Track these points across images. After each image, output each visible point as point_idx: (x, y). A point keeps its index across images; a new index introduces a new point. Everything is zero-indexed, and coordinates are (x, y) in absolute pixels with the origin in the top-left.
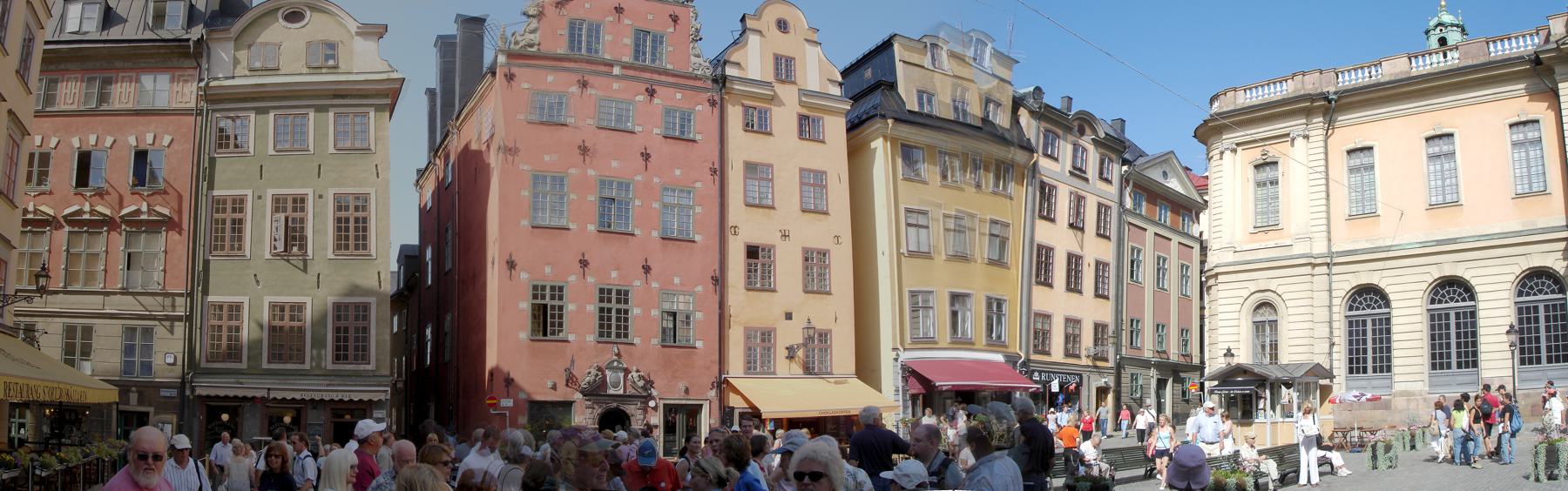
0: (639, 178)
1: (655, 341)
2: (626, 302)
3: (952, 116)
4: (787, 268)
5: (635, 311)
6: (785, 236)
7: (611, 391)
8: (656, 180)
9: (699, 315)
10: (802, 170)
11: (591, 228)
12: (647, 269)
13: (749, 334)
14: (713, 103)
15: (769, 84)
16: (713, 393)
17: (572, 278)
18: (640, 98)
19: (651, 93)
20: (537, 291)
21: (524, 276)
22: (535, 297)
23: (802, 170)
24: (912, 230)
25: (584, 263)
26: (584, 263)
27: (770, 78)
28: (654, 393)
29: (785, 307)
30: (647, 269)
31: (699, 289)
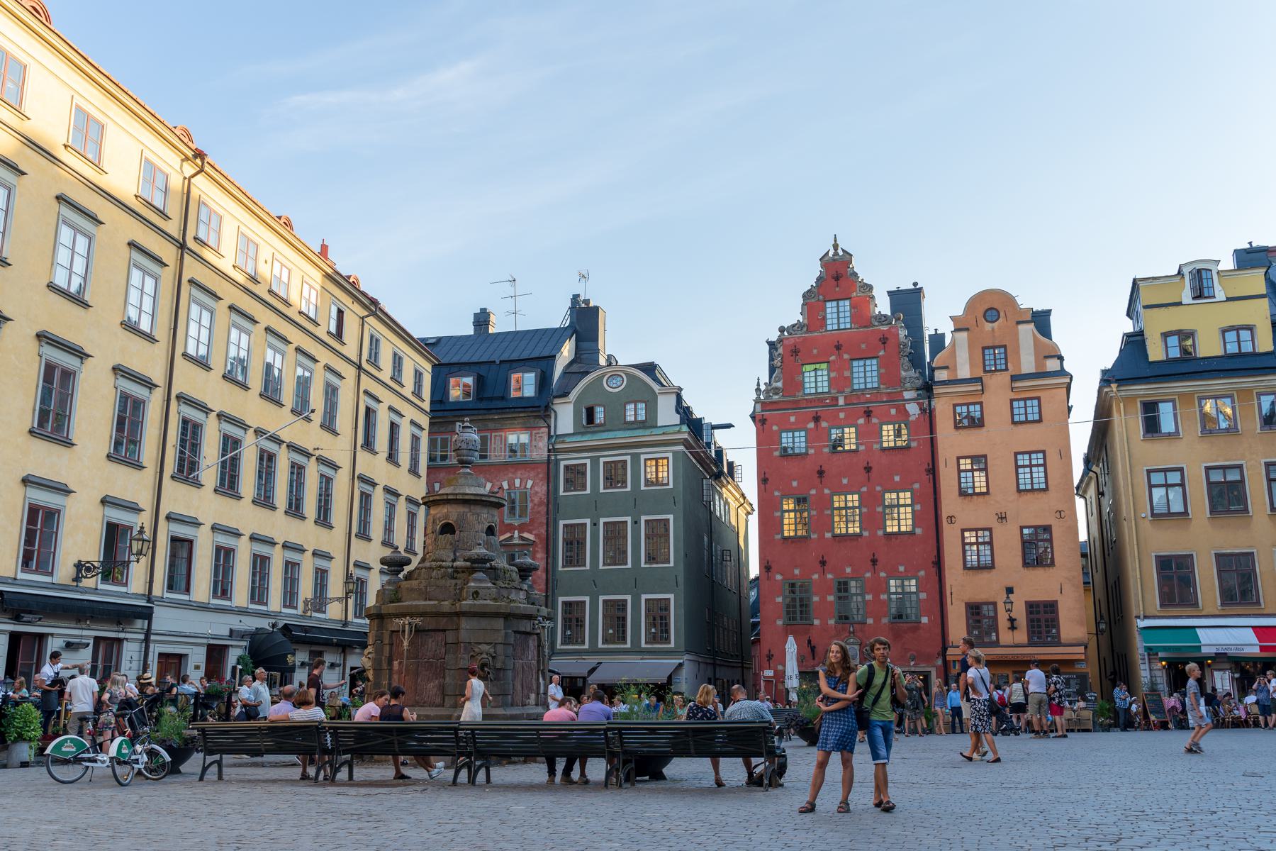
0: (864, 489)
1: (885, 620)
3: (1219, 352)
6: (1002, 518)
8: (878, 488)
9: (923, 596)
10: (1016, 454)
11: (828, 535)
12: (874, 562)
13: (974, 610)
15: (981, 379)
16: (940, 662)
18: (861, 421)
19: (868, 414)
21: (779, 577)
23: (1016, 454)
24: (1158, 493)
25: (823, 563)
26: (823, 563)
27: (980, 373)
30: (874, 562)
31: (922, 573)
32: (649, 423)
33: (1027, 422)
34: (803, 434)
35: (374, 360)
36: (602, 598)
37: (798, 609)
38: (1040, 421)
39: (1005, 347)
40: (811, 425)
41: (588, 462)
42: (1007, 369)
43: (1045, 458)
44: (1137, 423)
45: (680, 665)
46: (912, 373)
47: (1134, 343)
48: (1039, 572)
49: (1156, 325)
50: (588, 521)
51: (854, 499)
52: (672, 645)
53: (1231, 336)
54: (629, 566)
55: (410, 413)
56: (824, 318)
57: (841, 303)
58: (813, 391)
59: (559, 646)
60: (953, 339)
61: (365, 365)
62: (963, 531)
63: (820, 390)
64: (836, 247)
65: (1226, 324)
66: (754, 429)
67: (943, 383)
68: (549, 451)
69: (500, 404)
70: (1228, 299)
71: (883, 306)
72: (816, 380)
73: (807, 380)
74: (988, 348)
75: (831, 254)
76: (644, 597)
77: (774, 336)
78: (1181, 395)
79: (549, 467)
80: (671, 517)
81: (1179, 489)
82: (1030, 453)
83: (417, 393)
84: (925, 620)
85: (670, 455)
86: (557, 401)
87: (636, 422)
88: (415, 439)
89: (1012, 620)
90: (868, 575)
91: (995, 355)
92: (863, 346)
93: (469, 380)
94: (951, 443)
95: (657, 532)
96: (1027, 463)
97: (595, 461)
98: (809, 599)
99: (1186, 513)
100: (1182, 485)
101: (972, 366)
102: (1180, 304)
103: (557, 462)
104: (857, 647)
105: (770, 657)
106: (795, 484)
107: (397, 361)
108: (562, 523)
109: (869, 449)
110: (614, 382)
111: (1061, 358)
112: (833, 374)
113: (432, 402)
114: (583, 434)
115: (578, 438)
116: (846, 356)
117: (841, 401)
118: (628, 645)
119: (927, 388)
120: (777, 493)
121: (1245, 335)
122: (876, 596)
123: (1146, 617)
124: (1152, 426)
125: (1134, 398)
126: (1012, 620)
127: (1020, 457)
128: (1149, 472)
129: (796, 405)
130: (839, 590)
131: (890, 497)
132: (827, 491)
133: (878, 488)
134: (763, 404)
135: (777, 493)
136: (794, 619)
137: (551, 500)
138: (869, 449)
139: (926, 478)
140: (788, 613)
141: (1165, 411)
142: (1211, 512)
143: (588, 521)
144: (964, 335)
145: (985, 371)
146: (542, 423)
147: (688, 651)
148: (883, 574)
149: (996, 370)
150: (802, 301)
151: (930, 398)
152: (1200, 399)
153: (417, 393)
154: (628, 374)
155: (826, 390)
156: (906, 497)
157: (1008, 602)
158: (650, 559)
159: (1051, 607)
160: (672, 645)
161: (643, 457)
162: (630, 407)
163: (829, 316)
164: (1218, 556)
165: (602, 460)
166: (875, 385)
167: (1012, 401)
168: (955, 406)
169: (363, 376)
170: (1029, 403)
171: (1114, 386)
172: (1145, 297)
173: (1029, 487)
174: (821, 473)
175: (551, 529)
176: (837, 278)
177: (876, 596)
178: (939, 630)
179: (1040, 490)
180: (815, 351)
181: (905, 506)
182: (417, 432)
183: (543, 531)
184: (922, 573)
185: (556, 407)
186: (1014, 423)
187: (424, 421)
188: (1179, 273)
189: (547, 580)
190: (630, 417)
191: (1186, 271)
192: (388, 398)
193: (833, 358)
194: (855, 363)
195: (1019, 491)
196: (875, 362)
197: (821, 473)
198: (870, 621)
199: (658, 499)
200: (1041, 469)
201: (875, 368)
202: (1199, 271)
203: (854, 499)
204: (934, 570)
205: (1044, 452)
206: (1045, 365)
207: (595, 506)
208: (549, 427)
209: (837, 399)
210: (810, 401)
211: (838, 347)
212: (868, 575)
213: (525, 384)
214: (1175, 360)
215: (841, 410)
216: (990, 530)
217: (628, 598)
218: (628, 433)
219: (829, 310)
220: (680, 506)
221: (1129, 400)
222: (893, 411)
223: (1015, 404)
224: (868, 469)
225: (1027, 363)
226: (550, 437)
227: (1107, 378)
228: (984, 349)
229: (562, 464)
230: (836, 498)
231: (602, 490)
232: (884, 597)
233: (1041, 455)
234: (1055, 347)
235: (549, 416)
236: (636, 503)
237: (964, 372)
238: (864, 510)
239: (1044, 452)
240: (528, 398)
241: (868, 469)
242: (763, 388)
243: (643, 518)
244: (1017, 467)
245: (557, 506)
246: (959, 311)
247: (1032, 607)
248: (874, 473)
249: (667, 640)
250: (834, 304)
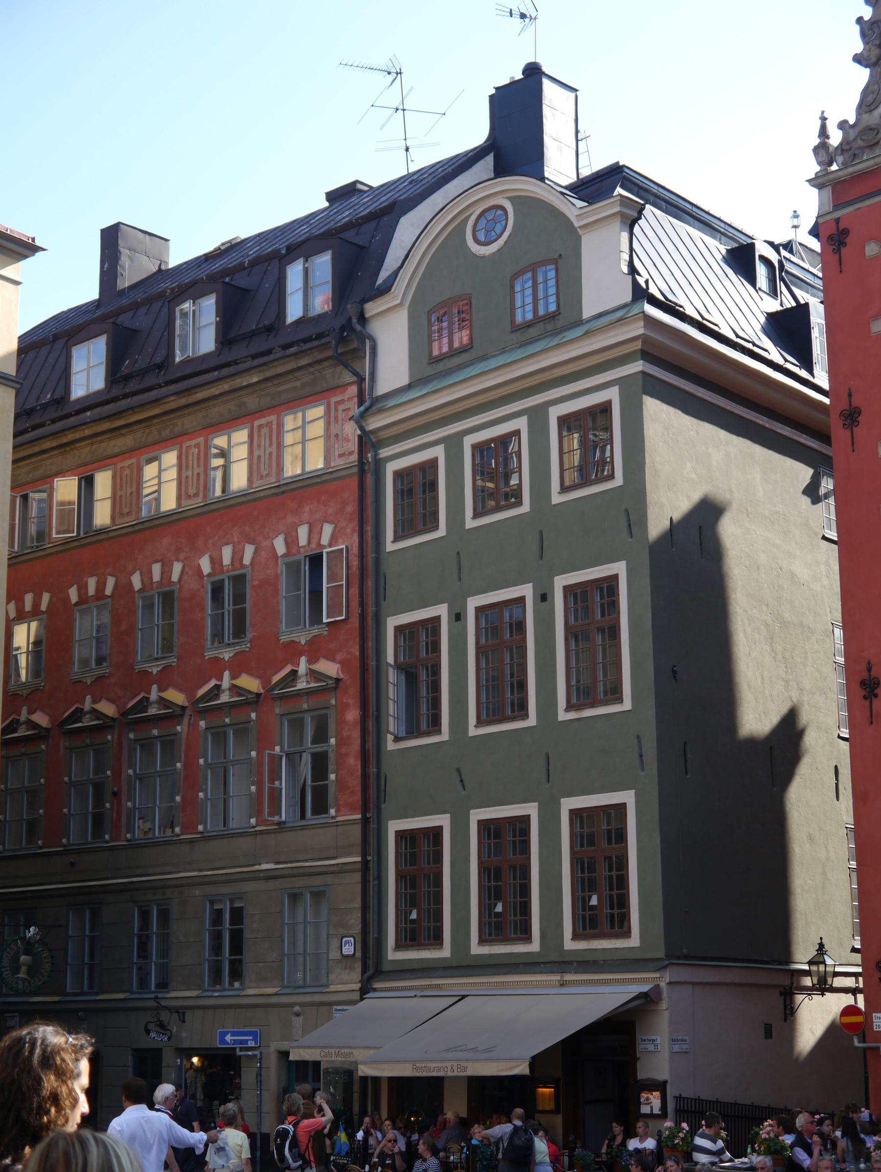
52: (634, 941)
59: (393, 955)
118: (535, 946)
143: (442, 611)
158: (582, 696)
160: (634, 941)
161: (555, 413)
189: (365, 776)
217: (531, 809)
242: (836, 138)
249: (619, 925)
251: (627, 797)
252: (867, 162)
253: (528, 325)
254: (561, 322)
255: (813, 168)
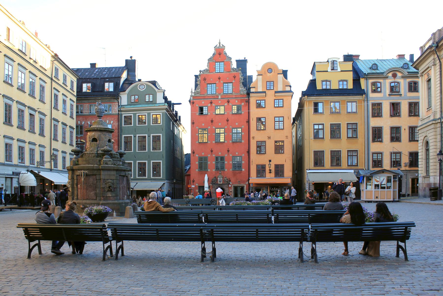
0: (226, 127)
1: (231, 170)
2: (223, 160)
4: (270, 147)
5: (226, 162)
6: (269, 138)
7: (219, 183)
8: (231, 127)
11: (214, 142)
12: (228, 151)
14: (246, 102)
16: (247, 183)
17: (209, 155)
18: (226, 104)
19: (228, 102)
20: (201, 159)
21: (197, 156)
22: (200, 160)
23: (275, 117)
25: (212, 151)
26: (212, 151)
27: (265, 90)
28: (231, 183)
29: (270, 158)
30: (228, 151)
31: (243, 155)
32: (154, 102)
33: (279, 107)
34: (206, 108)
35: (56, 77)
36: (137, 162)
37: (203, 166)
38: (283, 107)
39: (273, 82)
40: (209, 105)
41: (132, 115)
42: (273, 89)
43: (283, 119)
44: (312, 108)
45: (164, 184)
46: (243, 89)
47: (313, 83)
48: (279, 155)
49: (319, 78)
50: (132, 135)
51: (222, 130)
53: (341, 83)
54: (147, 151)
55: (70, 96)
56: (215, 68)
57: (221, 63)
58: (210, 93)
60: (257, 80)
61: (54, 78)
62: (257, 142)
63: (213, 93)
64: (220, 43)
65: (340, 79)
66: (190, 106)
67: (253, 92)
68: (119, 111)
69: (102, 93)
70: (341, 71)
71: (234, 65)
72: (211, 90)
73: (208, 89)
74: (268, 82)
75: (218, 46)
76: (152, 161)
77: (198, 74)
78: (325, 101)
79: (119, 116)
80: (161, 135)
81: (322, 130)
82: (279, 117)
83: (72, 89)
84: (243, 170)
85: (161, 113)
86: (121, 93)
87: (149, 101)
88: (72, 106)
89: (270, 170)
90: (226, 155)
91: (270, 84)
92: (228, 79)
93: (89, 85)
94: (255, 113)
95: (156, 139)
96: (278, 120)
97: (135, 115)
98: (206, 163)
99: (323, 138)
100: (323, 129)
101: (263, 87)
102: (327, 71)
103: (121, 115)
104: (222, 178)
105: (193, 181)
106: (203, 125)
107: (65, 77)
108: (123, 136)
109: (228, 113)
110: (142, 87)
111: (290, 86)
112: (217, 88)
113: (77, 92)
114: (131, 105)
115: (129, 107)
116: (222, 82)
117: (220, 97)
119: (248, 94)
120: (197, 128)
121: (345, 83)
122: (228, 162)
123: (309, 170)
124: (316, 110)
125: (311, 101)
126: (270, 170)
127: (276, 118)
128: (314, 124)
129: (204, 98)
130: (217, 160)
131: (234, 131)
132: (214, 127)
133: (231, 127)
134: (193, 97)
135: (197, 128)
136: (202, 169)
137: (120, 127)
138: (228, 113)
139: (246, 124)
140: (200, 167)
141: (320, 105)
142: (331, 138)
143: (132, 135)
144: (261, 76)
145: (267, 89)
146: (116, 101)
147: (167, 179)
148: (231, 155)
149: (270, 89)
150: (207, 62)
151: (248, 97)
152: (331, 102)
153: (72, 89)
154: (147, 85)
155: (215, 93)
156: (240, 130)
157: (270, 164)
158: (154, 149)
159: (282, 166)
160: (161, 177)
161: (151, 114)
162: (147, 96)
163: (216, 67)
164: (331, 151)
165: (137, 115)
166: (231, 92)
167: (275, 100)
168: (257, 100)
169: (53, 82)
170: (280, 101)
171: (306, 96)
172: (317, 69)
173: (278, 128)
174: (212, 121)
175: (120, 138)
176: (220, 54)
177: (228, 162)
178: (248, 173)
179: (281, 129)
180: (211, 80)
181: (239, 133)
182: (72, 103)
183: (117, 138)
184: (243, 155)
185: (121, 95)
186: (275, 107)
187: (75, 99)
188: (328, 61)
190: (147, 100)
191: (330, 61)
192: (62, 91)
193: (217, 82)
194: (225, 84)
195: (275, 129)
196: (231, 84)
197: (212, 121)
198: (226, 170)
199: (157, 129)
200: (282, 122)
201: (231, 86)
202: (334, 61)
203: (222, 130)
204: (247, 154)
205: (283, 117)
206: (285, 89)
207: (135, 131)
208: (118, 102)
209: (218, 96)
210: (209, 96)
211: (219, 78)
212: (226, 155)
213: (109, 87)
214: (324, 89)
215: (220, 100)
216: (265, 142)
218: (146, 105)
219: (216, 65)
220: (164, 131)
221: (309, 102)
222: (237, 101)
223: (276, 101)
224: (228, 120)
225: (280, 88)
226: (119, 106)
227: (304, 94)
228: (267, 82)
229: (123, 115)
230: (217, 130)
231: (137, 125)
232: (231, 162)
233: (282, 118)
234: (288, 83)
235: (119, 99)
236: (149, 130)
237: (260, 90)
238: (226, 134)
239: (283, 117)
240: (111, 92)
241: (228, 120)
242: (193, 91)
243: (152, 135)
244: (275, 121)
245: (121, 130)
246: (259, 68)
247: (277, 166)
248: (229, 122)
250: (219, 63)
251: (161, 161)
252: (197, 95)
253: (148, 102)
254: (153, 103)
255: (191, 94)
